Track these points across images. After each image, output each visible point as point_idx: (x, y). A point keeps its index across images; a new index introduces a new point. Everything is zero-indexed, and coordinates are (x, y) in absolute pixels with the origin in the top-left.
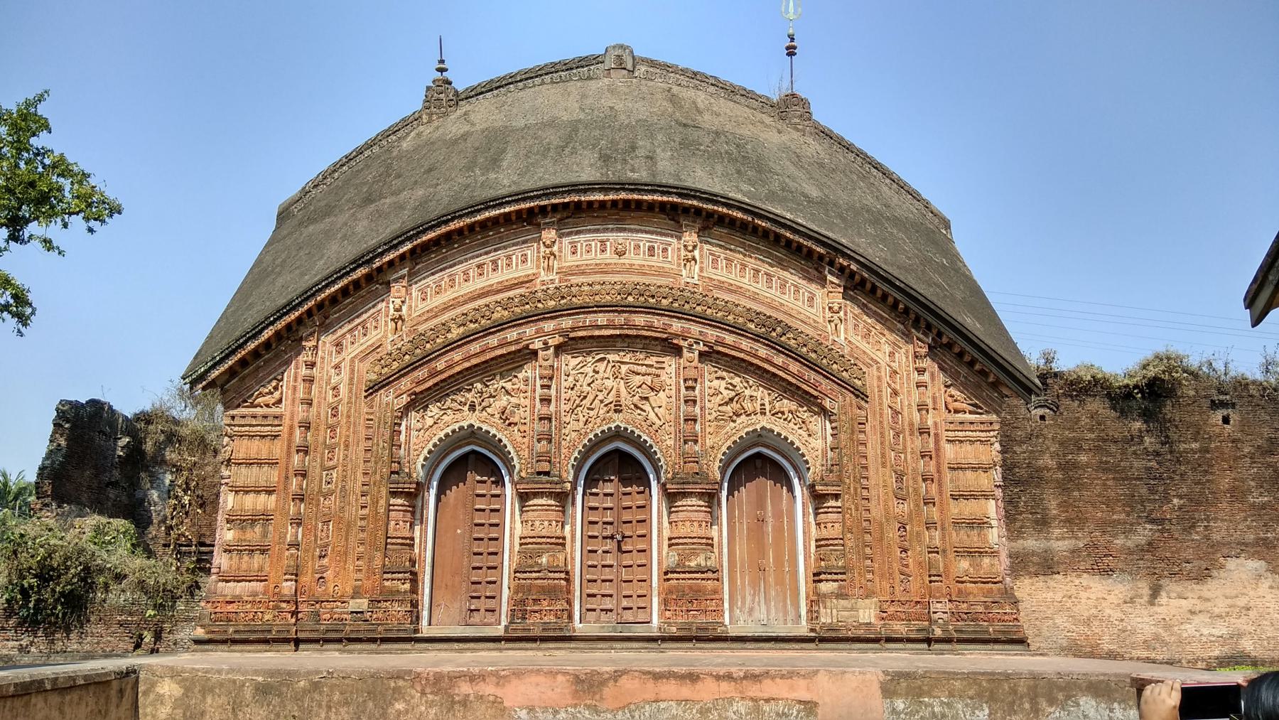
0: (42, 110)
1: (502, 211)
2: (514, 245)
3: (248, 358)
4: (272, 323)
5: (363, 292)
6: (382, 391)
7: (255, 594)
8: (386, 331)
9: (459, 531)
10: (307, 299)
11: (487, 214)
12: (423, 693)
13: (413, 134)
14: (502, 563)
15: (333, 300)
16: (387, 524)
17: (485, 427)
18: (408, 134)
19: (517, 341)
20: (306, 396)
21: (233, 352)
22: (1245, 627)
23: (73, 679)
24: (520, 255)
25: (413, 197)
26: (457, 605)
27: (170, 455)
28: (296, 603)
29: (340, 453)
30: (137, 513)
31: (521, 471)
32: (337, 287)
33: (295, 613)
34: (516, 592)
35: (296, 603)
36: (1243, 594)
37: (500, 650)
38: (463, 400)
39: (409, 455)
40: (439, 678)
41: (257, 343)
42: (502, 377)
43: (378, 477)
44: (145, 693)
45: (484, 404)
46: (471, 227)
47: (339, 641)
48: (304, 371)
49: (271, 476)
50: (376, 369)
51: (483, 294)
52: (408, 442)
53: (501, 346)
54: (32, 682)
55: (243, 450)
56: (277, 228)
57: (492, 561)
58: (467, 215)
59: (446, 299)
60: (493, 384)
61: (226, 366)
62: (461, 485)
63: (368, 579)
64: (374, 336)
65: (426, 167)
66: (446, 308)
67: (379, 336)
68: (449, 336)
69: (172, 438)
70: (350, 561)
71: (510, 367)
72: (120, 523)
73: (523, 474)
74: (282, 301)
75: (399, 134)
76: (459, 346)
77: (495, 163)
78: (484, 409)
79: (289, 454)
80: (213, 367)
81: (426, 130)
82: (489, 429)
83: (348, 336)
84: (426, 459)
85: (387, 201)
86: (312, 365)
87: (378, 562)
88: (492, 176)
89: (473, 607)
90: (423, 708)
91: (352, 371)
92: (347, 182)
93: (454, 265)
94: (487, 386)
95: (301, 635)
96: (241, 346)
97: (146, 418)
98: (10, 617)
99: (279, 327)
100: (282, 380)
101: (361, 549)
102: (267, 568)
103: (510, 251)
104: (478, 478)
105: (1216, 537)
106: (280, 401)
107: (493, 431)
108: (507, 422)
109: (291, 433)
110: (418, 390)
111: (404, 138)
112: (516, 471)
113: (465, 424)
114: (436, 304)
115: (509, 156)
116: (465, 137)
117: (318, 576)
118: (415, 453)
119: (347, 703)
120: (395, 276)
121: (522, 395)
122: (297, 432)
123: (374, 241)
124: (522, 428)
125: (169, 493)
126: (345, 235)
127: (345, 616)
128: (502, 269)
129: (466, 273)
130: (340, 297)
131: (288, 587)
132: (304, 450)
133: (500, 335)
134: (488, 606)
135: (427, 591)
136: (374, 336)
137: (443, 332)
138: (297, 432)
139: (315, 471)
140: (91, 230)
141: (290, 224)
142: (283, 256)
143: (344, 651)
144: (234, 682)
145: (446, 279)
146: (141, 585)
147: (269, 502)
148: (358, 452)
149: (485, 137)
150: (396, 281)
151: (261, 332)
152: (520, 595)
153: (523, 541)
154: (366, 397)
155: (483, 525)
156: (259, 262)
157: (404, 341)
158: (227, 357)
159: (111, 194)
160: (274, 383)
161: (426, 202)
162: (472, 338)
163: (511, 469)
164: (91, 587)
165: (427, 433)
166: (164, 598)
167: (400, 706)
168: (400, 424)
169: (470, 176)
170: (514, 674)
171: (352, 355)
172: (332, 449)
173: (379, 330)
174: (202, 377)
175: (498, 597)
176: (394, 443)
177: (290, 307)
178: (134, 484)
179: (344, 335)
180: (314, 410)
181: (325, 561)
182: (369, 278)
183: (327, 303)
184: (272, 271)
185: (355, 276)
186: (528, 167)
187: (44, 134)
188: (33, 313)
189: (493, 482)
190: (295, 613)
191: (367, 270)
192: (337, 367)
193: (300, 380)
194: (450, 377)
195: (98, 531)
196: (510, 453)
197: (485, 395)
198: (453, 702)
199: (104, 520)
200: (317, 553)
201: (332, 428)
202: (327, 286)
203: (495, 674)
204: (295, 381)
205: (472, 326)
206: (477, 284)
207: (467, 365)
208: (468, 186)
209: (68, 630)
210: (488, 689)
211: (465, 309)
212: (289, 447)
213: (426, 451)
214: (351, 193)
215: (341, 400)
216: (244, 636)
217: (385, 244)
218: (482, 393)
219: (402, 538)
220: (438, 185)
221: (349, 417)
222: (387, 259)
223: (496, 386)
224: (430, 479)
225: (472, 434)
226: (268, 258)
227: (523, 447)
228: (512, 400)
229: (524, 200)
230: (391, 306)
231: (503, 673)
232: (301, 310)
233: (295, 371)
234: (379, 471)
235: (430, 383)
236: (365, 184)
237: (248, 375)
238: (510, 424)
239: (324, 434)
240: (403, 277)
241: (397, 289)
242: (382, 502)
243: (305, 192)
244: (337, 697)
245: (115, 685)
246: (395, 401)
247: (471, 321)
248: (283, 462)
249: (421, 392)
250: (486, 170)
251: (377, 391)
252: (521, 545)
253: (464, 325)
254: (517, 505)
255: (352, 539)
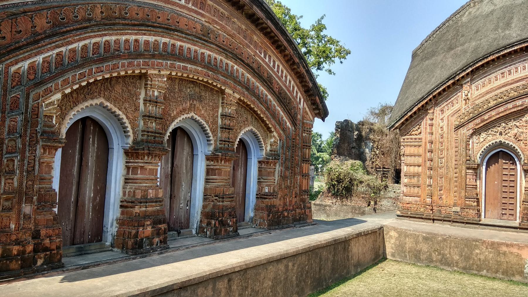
0: (323, 22)
1: (513, 49)
2: (519, 62)
3: (408, 118)
4: (417, 105)
5: (451, 89)
6: (461, 129)
7: (416, 201)
8: (461, 104)
9: (496, 183)
10: (429, 95)
11: (506, 51)
12: (487, 248)
13: (467, 13)
14: (516, 197)
15: (440, 94)
16: (466, 180)
17: (507, 142)
18: (465, 13)
19: (521, 105)
20: (431, 131)
21: (403, 117)
23: (368, 231)
24: (522, 66)
25: (471, 46)
26: (496, 211)
27: (371, 137)
28: (432, 206)
29: (445, 153)
30: (361, 157)
31: (525, 160)
32: (441, 89)
33: (432, 210)
34: (524, 210)
35: (432, 206)
37: (517, 232)
38: (497, 130)
39: (473, 153)
40: (493, 244)
41: (411, 113)
42: (514, 120)
43: (461, 162)
44: (386, 234)
45: (506, 132)
46: (498, 58)
47: (450, 221)
48: (429, 122)
49: (420, 160)
50: (458, 120)
51: (504, 85)
52: (473, 148)
53: (514, 108)
54: (359, 233)
55: (408, 151)
56: (412, 61)
57: (512, 195)
58: (496, 53)
59: (487, 89)
60: (510, 124)
61: (401, 122)
62: (496, 164)
63: (459, 200)
64: (456, 107)
65: (475, 31)
66: (488, 93)
67: (458, 107)
68: (489, 105)
69: (371, 130)
70: (451, 192)
71: (518, 116)
72: (358, 162)
73: (526, 161)
74: (420, 97)
75: (460, 14)
76: (494, 109)
77: (508, 25)
78: (506, 134)
79: (425, 153)
80: (396, 122)
81: (473, 10)
82: (509, 142)
83: (446, 107)
84: (481, 155)
85: (459, 48)
86: (433, 119)
87: (463, 194)
88: (507, 32)
89: (503, 213)
90: (487, 253)
91: (448, 121)
92: (440, 39)
93: (491, 74)
94: (507, 124)
95: (435, 218)
96: (406, 114)
97: (362, 123)
98: (329, 193)
99: (419, 106)
100: (421, 125)
101: (456, 189)
102: (420, 192)
103: (517, 65)
104: (504, 161)
106: (421, 133)
107: (511, 143)
108: (518, 139)
109: (426, 145)
110: (476, 127)
111: (463, 15)
112: (522, 160)
113: (498, 141)
114: (483, 91)
115: (515, 20)
116: (492, 12)
117: (439, 197)
118: (476, 152)
119: (457, 247)
120: (465, 82)
121: (524, 128)
122: (428, 144)
123: (455, 69)
124: (525, 142)
125: (372, 150)
126: (442, 66)
127: (451, 212)
128: (513, 74)
129: (495, 77)
130: (442, 92)
131: (429, 200)
132: (431, 151)
133: (514, 103)
134: (510, 213)
135: (483, 205)
136: (456, 107)
137: (487, 103)
138: (428, 144)
139: (436, 159)
140: (341, 62)
141: (418, 59)
142: (417, 75)
143: (452, 225)
144: (416, 234)
145: (487, 81)
146: (368, 185)
147: (419, 170)
148: (452, 152)
149: (502, 11)
150: (465, 84)
151: (413, 109)
152: (526, 211)
153: (526, 189)
154: (455, 131)
155: (507, 181)
156: (407, 77)
157: (470, 107)
158: (401, 118)
159: (346, 48)
160: (418, 126)
161: (477, 49)
162: (500, 105)
163: (520, 160)
164: (353, 185)
165: (481, 144)
166: (377, 190)
167: (477, 251)
168: (469, 141)
169: (496, 34)
170: (526, 246)
171: (448, 114)
172: (442, 151)
173: (458, 104)
174: (393, 126)
175: (515, 209)
176: (467, 148)
177: (423, 99)
178: (360, 147)
179: (444, 107)
180: (434, 136)
181: (442, 192)
182: (454, 84)
183: (437, 95)
184: (414, 82)
185: (448, 84)
186: (525, 25)
187: (324, 30)
188: (328, 96)
189: (511, 163)
190: (432, 210)
191: (453, 81)
192: (442, 119)
193: (428, 125)
194: (490, 122)
195: (352, 166)
196: (519, 153)
197: (507, 128)
198: (499, 253)
199: (354, 161)
200: (439, 189)
201: (442, 143)
202: (437, 89)
203: (518, 245)
204: (426, 125)
205: (500, 100)
206: (502, 81)
207: (498, 116)
208: (496, 39)
209: (347, 198)
210: (515, 250)
211: (496, 92)
212: (425, 150)
213: (481, 152)
214: (442, 45)
215: (444, 132)
216: (414, 216)
217: (460, 70)
218: (505, 127)
219: (472, 185)
220: (481, 39)
221: (448, 138)
222: (461, 76)
223: (511, 124)
224: (483, 162)
225: (501, 144)
226: (411, 76)
227: (526, 150)
228: (520, 130)
229: (524, 42)
230: (464, 94)
231: (521, 245)
232: (427, 99)
233: (426, 122)
234: (461, 160)
235: (482, 125)
236: (447, 40)
237: (409, 124)
238: (519, 140)
239: (438, 145)
240: (468, 82)
241: (465, 86)
242: (464, 172)
243: (422, 45)
244: (453, 245)
245: (378, 232)
246: (467, 132)
247: (499, 98)
248: (423, 156)
249: (478, 128)
250: (504, 30)
251: (459, 129)
252: (525, 190)
253: (496, 100)
254: (523, 174)
255: (452, 185)
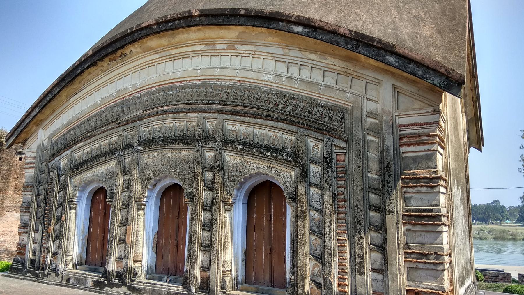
22: (8, 239)
36: (10, 226)
105: (5, 204)
